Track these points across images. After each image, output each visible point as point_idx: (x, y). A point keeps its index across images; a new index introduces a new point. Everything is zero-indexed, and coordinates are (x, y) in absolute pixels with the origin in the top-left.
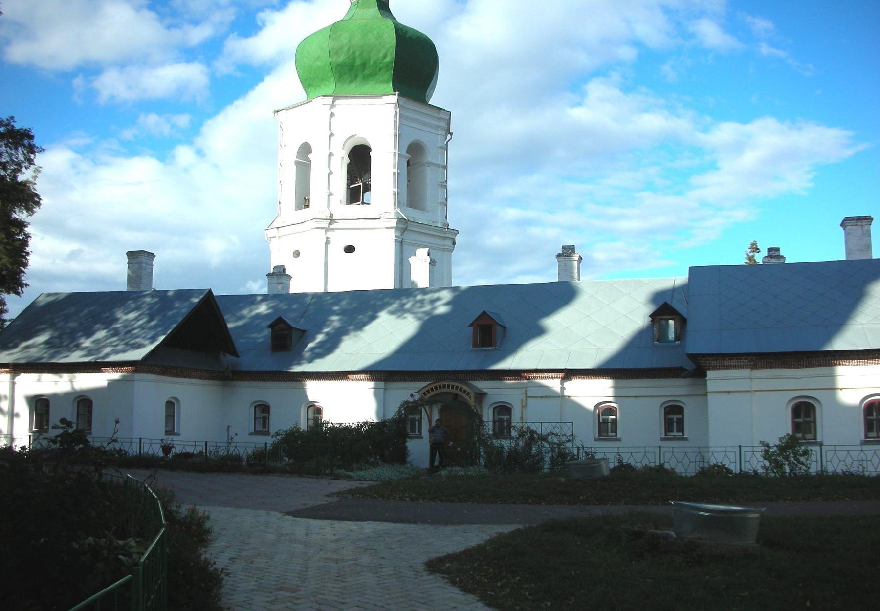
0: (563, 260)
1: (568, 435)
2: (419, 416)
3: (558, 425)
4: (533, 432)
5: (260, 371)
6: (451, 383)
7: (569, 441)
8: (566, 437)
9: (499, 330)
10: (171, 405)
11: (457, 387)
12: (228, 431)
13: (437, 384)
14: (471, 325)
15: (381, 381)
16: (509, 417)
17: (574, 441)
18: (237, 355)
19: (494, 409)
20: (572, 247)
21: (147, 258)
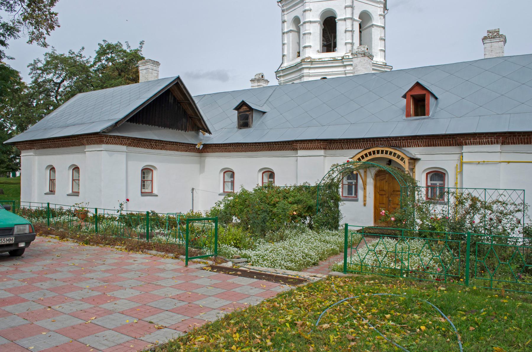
0: (490, 41)
1: (517, 204)
2: (355, 181)
3: (505, 193)
4: (474, 200)
5: (226, 144)
6: (385, 149)
7: (519, 211)
8: (514, 207)
9: (432, 100)
10: (146, 171)
11: (391, 153)
12: (192, 192)
13: (371, 150)
14: (405, 96)
15: (321, 149)
16: (442, 182)
17: (526, 212)
18: (210, 133)
19: (427, 174)
20: (497, 30)
21: (153, 65)
